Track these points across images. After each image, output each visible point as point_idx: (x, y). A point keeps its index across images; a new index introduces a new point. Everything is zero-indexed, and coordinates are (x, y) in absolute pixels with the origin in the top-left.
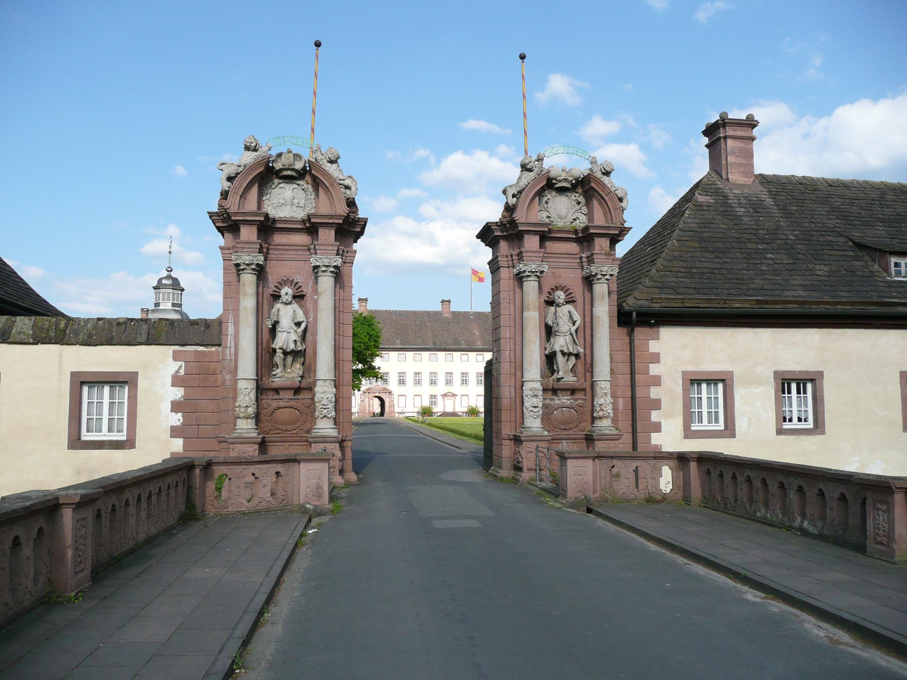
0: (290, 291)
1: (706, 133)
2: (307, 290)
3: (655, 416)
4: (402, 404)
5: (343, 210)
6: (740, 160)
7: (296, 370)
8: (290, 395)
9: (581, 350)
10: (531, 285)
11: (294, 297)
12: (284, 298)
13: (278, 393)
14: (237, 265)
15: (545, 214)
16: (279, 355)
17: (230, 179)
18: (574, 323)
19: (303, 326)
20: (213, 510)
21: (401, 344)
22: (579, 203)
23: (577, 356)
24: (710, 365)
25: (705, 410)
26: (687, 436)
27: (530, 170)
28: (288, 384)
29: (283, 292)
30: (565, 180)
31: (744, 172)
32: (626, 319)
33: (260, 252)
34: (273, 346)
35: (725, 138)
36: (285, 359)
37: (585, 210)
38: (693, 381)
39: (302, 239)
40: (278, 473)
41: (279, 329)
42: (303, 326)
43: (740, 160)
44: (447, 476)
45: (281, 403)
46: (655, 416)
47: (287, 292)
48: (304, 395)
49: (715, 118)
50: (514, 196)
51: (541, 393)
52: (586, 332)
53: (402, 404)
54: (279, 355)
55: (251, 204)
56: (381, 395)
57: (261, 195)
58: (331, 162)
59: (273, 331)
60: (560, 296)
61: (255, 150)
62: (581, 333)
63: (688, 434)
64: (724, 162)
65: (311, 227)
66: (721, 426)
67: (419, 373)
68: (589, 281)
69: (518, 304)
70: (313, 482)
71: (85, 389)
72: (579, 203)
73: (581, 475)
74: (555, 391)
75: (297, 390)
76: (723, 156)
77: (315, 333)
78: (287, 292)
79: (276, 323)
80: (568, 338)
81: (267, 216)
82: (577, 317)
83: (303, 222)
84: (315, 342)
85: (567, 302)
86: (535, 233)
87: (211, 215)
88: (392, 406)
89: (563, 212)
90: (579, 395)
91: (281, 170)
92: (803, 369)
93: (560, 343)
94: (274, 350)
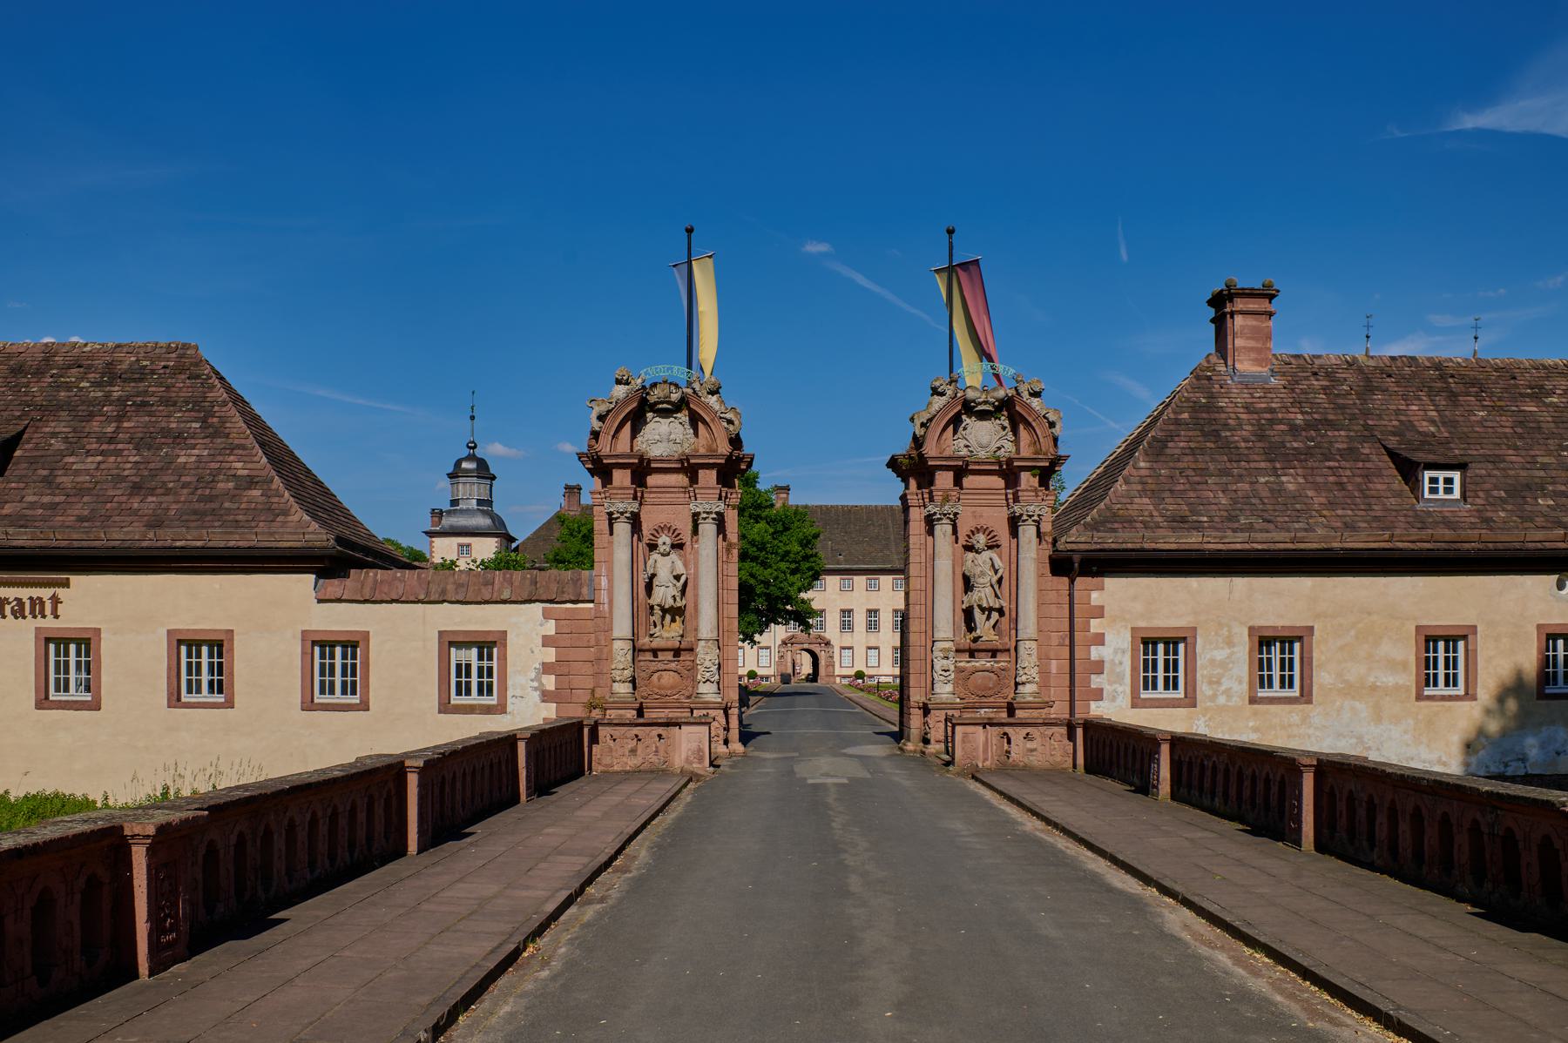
0: (668, 541)
1: (1211, 303)
2: (686, 536)
3: (1096, 681)
4: (847, 662)
5: (724, 448)
6: (1252, 344)
7: (676, 629)
8: (669, 655)
9: (1005, 604)
10: (943, 530)
11: (673, 546)
12: (662, 549)
13: (655, 656)
14: (610, 514)
15: (962, 443)
16: (657, 610)
17: (601, 418)
18: (996, 572)
19: (683, 579)
20: (600, 768)
21: (847, 562)
22: (1004, 428)
23: (1001, 611)
24: (1166, 620)
25: (1161, 674)
26: (1133, 706)
27: (942, 394)
28: (669, 644)
29: (660, 541)
30: (986, 402)
31: (1256, 360)
32: (1061, 565)
33: (635, 498)
34: (651, 602)
35: (1232, 314)
36: (663, 618)
37: (1010, 436)
38: (1145, 642)
39: (681, 479)
40: (660, 736)
41: (656, 582)
42: (683, 579)
43: (1252, 344)
44: (849, 751)
45: (661, 666)
46: (1096, 681)
47: (664, 540)
48: (684, 656)
49: (1219, 286)
50: (923, 425)
51: (952, 654)
52: (1006, 582)
53: (847, 662)
54: (657, 610)
55: (623, 445)
56: (812, 647)
57: (634, 435)
58: (712, 393)
59: (649, 588)
60: (981, 539)
61: (627, 383)
62: (1005, 583)
63: (1136, 703)
64: (1230, 346)
65: (689, 468)
66: (1180, 693)
67: (876, 611)
68: (1014, 523)
69: (930, 551)
70: (694, 745)
71: (453, 650)
72: (1004, 428)
73: (977, 744)
74: (972, 653)
75: (677, 652)
76: (1230, 338)
77: (696, 587)
78: (664, 540)
79: (654, 575)
80: (989, 590)
81: (641, 458)
82: (998, 563)
83: (681, 461)
84: (696, 596)
85: (990, 548)
86: (947, 468)
87: (580, 456)
88: (831, 665)
89: (984, 441)
90: (1000, 657)
91: (656, 403)
92: (1288, 624)
93: (983, 595)
94: (652, 608)
